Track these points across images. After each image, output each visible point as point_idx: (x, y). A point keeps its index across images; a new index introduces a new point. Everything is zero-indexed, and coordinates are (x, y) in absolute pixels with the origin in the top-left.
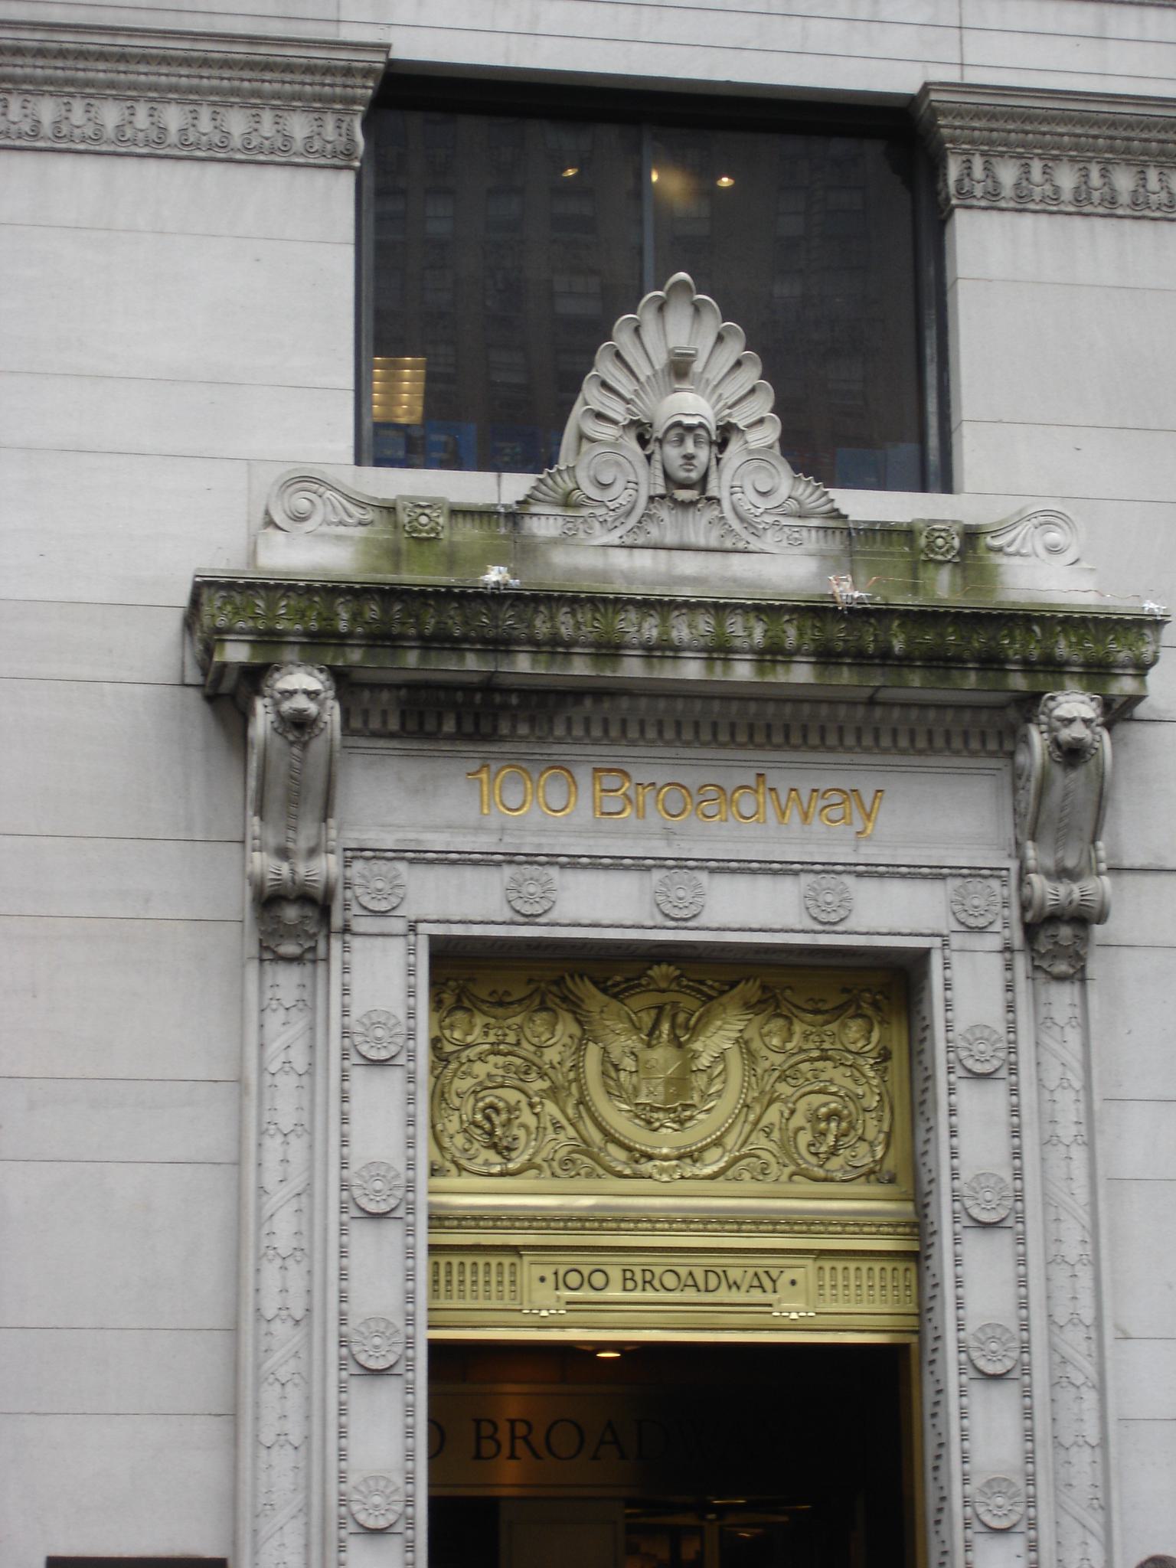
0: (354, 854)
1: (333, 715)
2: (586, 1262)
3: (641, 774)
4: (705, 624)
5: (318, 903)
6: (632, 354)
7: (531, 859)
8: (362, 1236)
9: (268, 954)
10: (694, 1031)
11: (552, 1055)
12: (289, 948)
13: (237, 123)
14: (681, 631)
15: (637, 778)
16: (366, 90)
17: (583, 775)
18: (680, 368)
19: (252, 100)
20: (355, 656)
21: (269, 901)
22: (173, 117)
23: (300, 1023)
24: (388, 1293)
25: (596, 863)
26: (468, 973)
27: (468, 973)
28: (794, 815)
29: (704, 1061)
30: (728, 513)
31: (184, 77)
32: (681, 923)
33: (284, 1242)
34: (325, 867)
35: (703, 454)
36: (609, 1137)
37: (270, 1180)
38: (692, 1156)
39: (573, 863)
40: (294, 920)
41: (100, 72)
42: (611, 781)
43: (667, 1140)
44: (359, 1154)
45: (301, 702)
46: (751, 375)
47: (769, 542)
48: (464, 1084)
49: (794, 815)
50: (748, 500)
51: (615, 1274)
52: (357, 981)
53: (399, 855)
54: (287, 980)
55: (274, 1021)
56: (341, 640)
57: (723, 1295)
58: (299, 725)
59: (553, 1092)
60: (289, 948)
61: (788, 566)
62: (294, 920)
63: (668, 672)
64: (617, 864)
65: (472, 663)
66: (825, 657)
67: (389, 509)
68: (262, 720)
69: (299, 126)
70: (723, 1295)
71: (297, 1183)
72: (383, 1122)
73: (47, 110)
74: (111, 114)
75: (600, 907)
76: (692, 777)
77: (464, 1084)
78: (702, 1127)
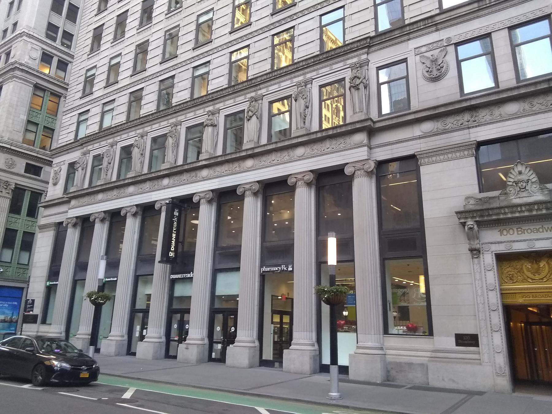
0: (483, 244)
1: (476, 227)
2: (526, 294)
3: (524, 228)
4: (527, 207)
5: (478, 251)
6: (513, 172)
7: (508, 242)
8: (490, 293)
9: (473, 258)
10: (540, 262)
11: (518, 267)
12: (475, 257)
13: (458, 154)
14: (524, 209)
15: (524, 228)
16: (474, 146)
17: (515, 230)
18: (520, 173)
19: (459, 151)
20: (477, 219)
21: (471, 250)
22: (450, 156)
23: (478, 266)
24: (495, 299)
25: (517, 241)
26: (501, 258)
27: (501, 258)
28: (549, 231)
29: (542, 266)
30: (530, 191)
31: (453, 150)
32: (531, 248)
33: (480, 294)
34: (478, 246)
35: (524, 184)
36: (528, 277)
37: (477, 286)
38: (542, 279)
39: (514, 241)
40: (475, 252)
41: (440, 152)
42: (519, 230)
43: (537, 277)
44: (488, 282)
45: (470, 226)
46: (531, 172)
47: (537, 194)
48: (505, 272)
49: (549, 231)
50: (533, 189)
51: (531, 296)
52: (485, 260)
53: (489, 243)
54: (476, 260)
55: (475, 266)
56: (475, 217)
57: (548, 298)
58: (471, 228)
59: (519, 272)
60: (475, 257)
61: (539, 197)
62: (475, 252)
63: (522, 214)
64: (521, 241)
65: (494, 217)
66: (547, 209)
67: (480, 199)
68: (466, 228)
69: (466, 153)
70: (548, 298)
71: (480, 286)
72: (492, 277)
73: (434, 159)
74: (442, 157)
75: (520, 247)
76: (532, 228)
77: (505, 272)
78: (543, 275)
